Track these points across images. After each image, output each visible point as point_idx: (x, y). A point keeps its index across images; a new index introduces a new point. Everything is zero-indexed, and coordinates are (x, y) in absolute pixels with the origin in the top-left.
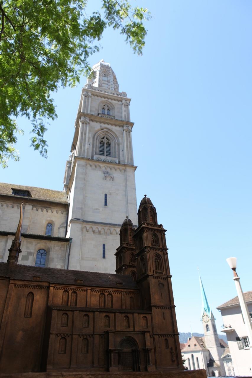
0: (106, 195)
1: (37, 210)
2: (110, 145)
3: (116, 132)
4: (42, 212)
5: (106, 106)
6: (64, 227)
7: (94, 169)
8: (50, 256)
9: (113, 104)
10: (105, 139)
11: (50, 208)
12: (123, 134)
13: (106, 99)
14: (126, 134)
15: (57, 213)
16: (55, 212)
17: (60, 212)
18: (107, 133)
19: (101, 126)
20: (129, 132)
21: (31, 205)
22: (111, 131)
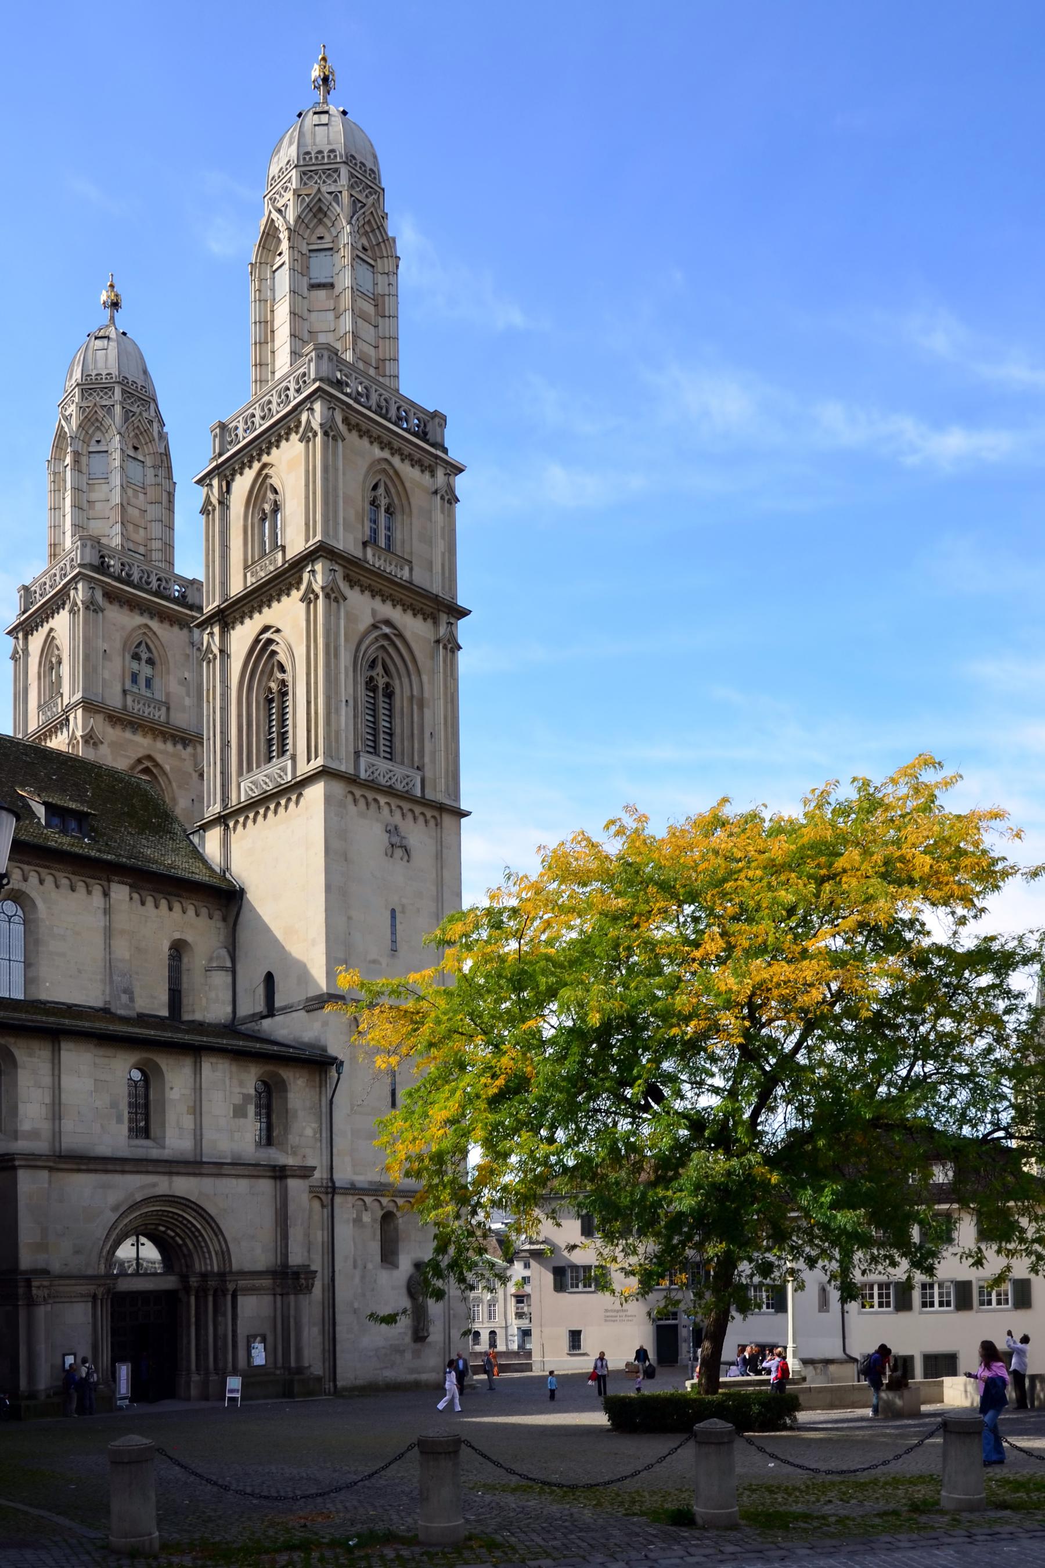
0: (393, 911)
1: (143, 903)
4: (155, 911)
5: (381, 490)
6: (222, 968)
7: (362, 815)
8: (290, 1106)
9: (408, 485)
11: (179, 896)
12: (433, 656)
13: (386, 454)
15: (197, 915)
16: (191, 911)
17: (204, 911)
18: (385, 643)
19: (374, 613)
20: (453, 651)
21: (125, 884)
22: (400, 636)
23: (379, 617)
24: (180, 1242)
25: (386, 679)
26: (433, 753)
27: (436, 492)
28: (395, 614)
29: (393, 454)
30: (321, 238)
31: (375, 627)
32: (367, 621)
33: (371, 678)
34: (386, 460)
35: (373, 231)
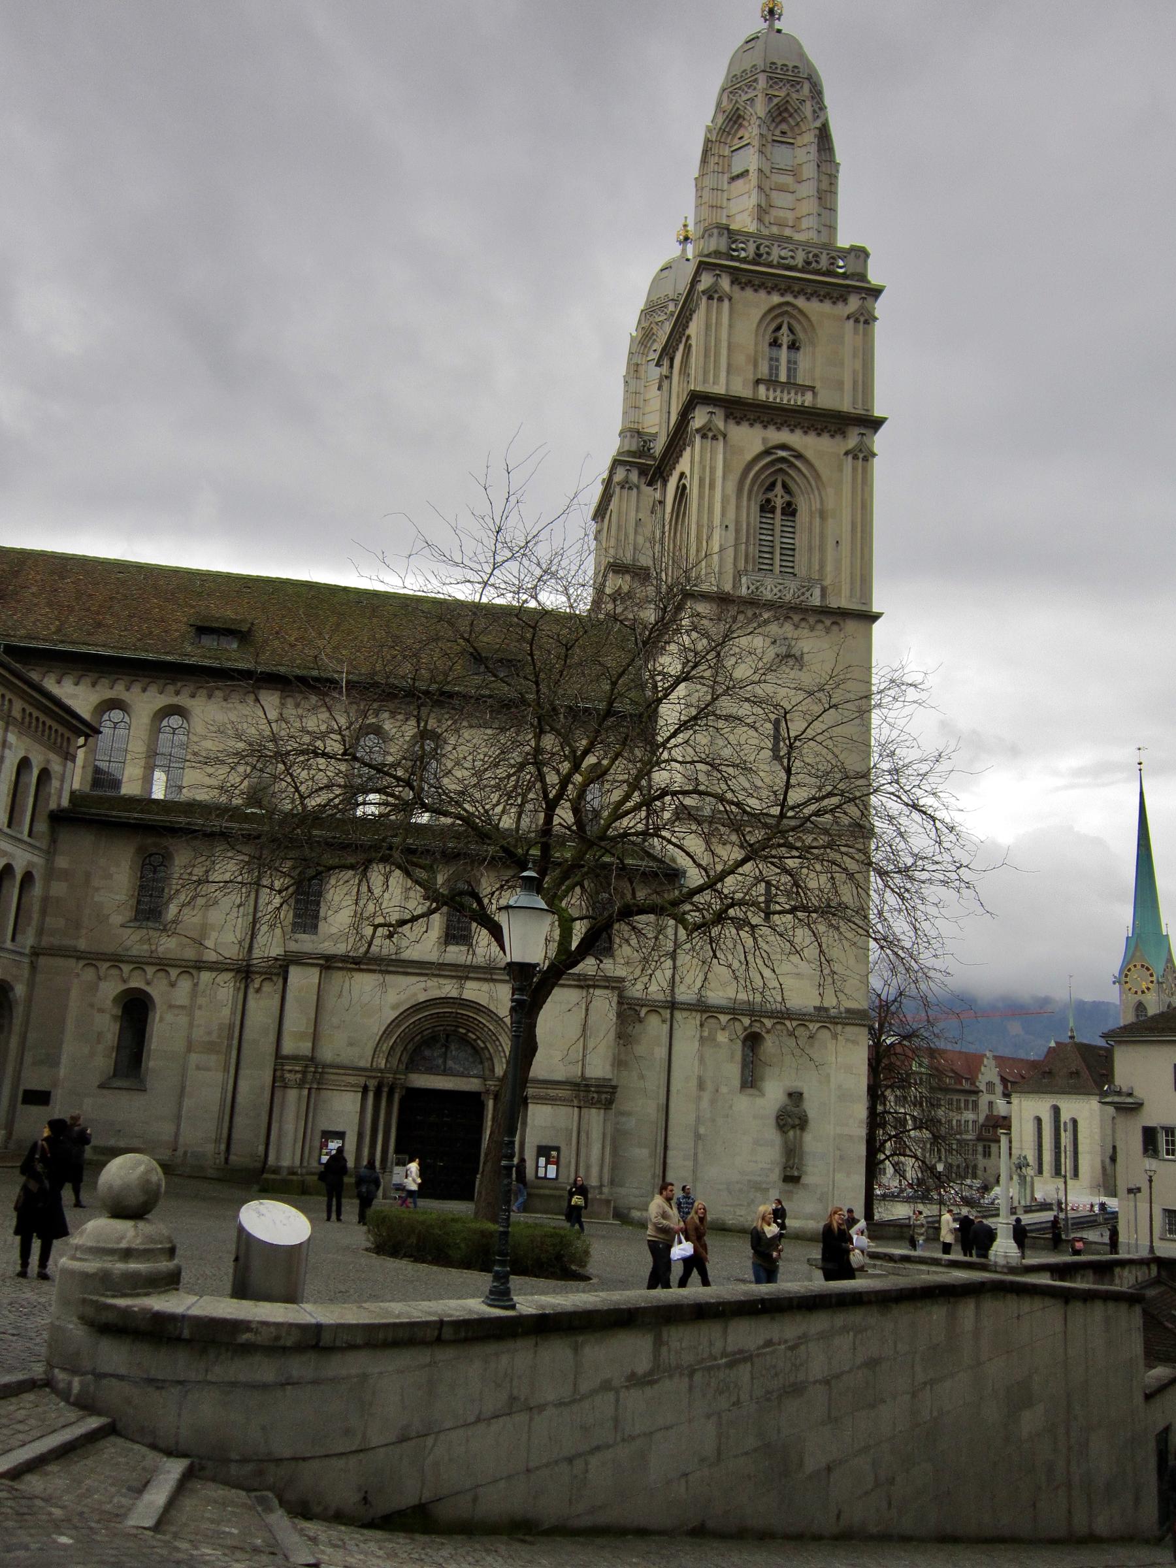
2: (793, 513)
3: (817, 463)
5: (785, 329)
9: (813, 319)
10: (779, 488)
14: (854, 469)
18: (784, 466)
19: (764, 440)
22: (799, 456)
23: (771, 444)
24: (482, 1045)
25: (787, 498)
26: (838, 561)
27: (848, 318)
28: (784, 436)
29: (795, 297)
30: (741, 138)
31: (767, 452)
32: (758, 448)
33: (768, 501)
34: (788, 304)
35: (791, 115)
